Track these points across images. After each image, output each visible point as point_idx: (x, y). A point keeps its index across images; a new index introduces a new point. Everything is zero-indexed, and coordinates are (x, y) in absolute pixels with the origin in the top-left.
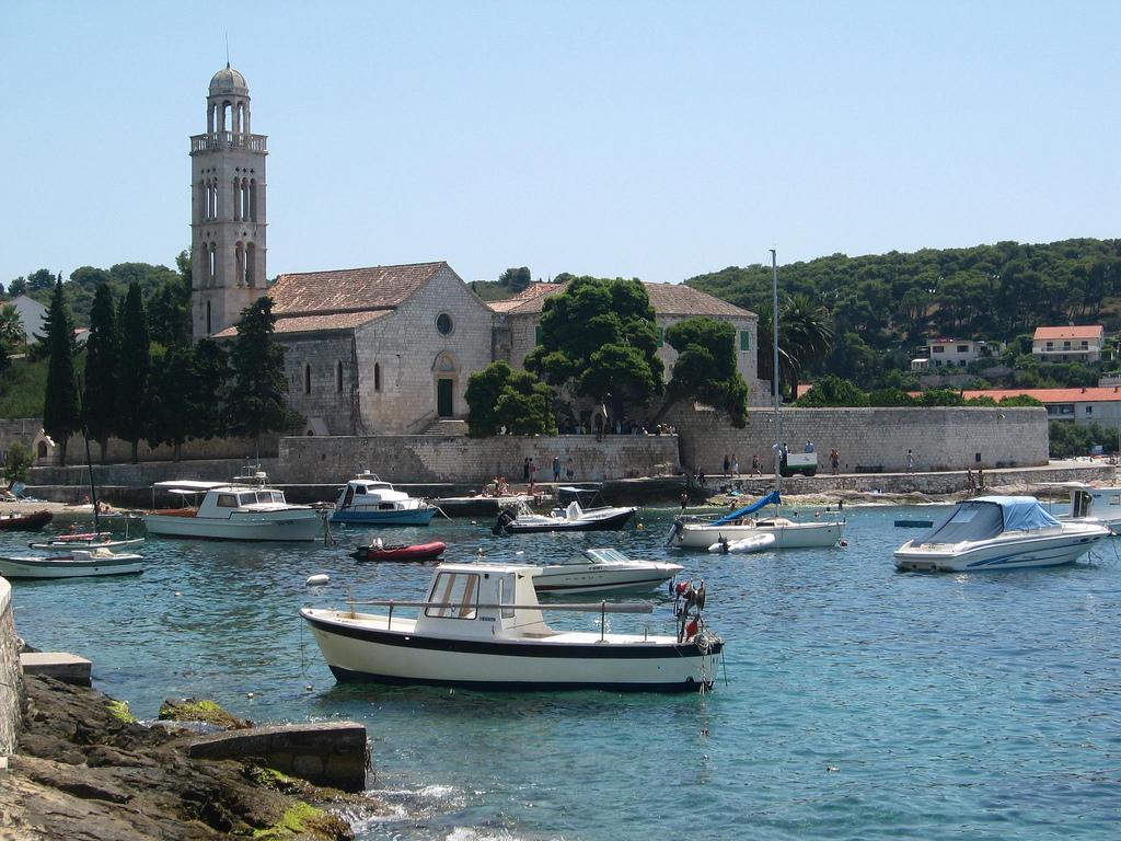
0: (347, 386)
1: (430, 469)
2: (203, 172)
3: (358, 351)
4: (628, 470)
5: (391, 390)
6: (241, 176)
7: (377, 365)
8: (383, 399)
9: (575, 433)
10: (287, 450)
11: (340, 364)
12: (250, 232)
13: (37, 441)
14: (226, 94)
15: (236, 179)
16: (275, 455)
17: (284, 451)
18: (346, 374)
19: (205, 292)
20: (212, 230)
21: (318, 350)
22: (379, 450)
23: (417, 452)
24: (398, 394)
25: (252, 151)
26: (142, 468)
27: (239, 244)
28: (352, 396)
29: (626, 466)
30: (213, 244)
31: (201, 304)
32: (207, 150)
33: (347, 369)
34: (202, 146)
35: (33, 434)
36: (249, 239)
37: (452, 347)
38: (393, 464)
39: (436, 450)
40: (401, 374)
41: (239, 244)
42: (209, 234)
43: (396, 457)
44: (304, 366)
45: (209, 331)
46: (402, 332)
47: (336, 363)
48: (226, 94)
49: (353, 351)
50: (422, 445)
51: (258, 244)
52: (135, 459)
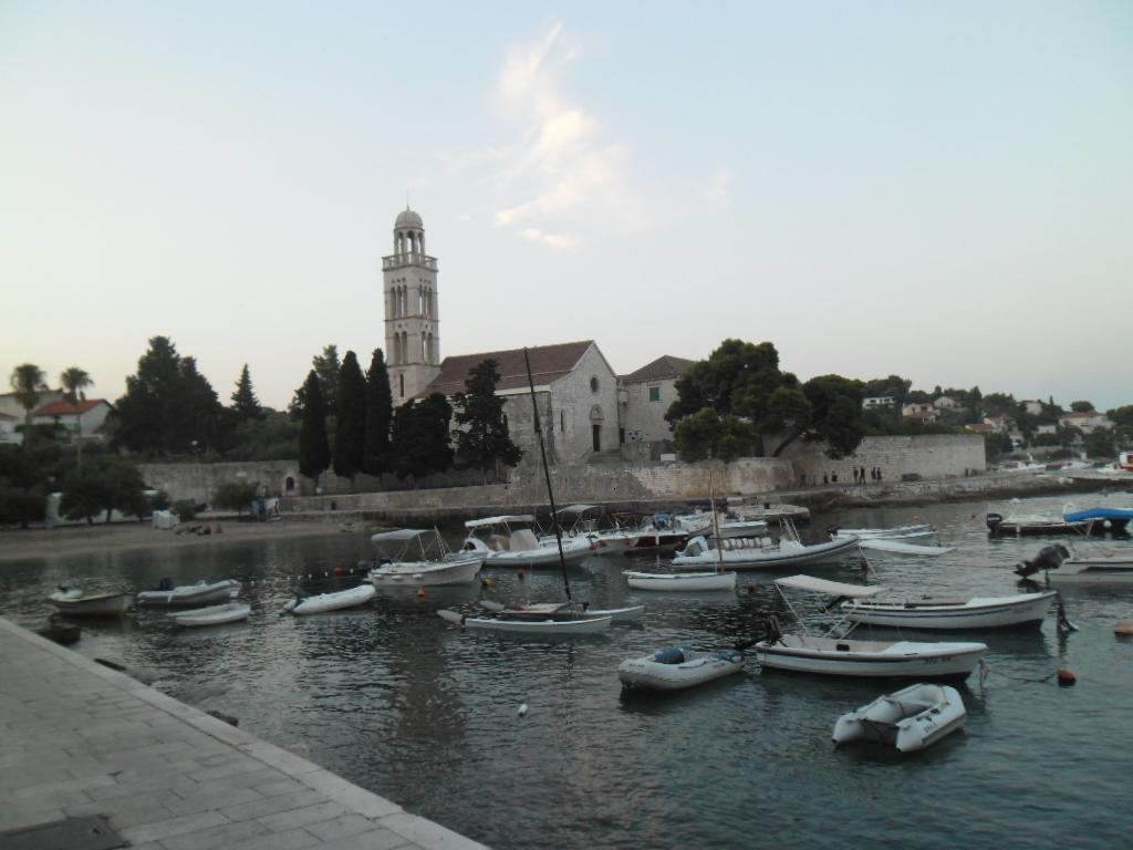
8: (566, 438)
9: (706, 458)
12: (430, 325)
14: (409, 230)
20: (403, 323)
25: (427, 267)
27: (423, 333)
32: (392, 266)
33: (543, 415)
34: (387, 266)
35: (281, 473)
36: (428, 330)
37: (599, 402)
43: (617, 479)
48: (409, 230)
49: (549, 403)
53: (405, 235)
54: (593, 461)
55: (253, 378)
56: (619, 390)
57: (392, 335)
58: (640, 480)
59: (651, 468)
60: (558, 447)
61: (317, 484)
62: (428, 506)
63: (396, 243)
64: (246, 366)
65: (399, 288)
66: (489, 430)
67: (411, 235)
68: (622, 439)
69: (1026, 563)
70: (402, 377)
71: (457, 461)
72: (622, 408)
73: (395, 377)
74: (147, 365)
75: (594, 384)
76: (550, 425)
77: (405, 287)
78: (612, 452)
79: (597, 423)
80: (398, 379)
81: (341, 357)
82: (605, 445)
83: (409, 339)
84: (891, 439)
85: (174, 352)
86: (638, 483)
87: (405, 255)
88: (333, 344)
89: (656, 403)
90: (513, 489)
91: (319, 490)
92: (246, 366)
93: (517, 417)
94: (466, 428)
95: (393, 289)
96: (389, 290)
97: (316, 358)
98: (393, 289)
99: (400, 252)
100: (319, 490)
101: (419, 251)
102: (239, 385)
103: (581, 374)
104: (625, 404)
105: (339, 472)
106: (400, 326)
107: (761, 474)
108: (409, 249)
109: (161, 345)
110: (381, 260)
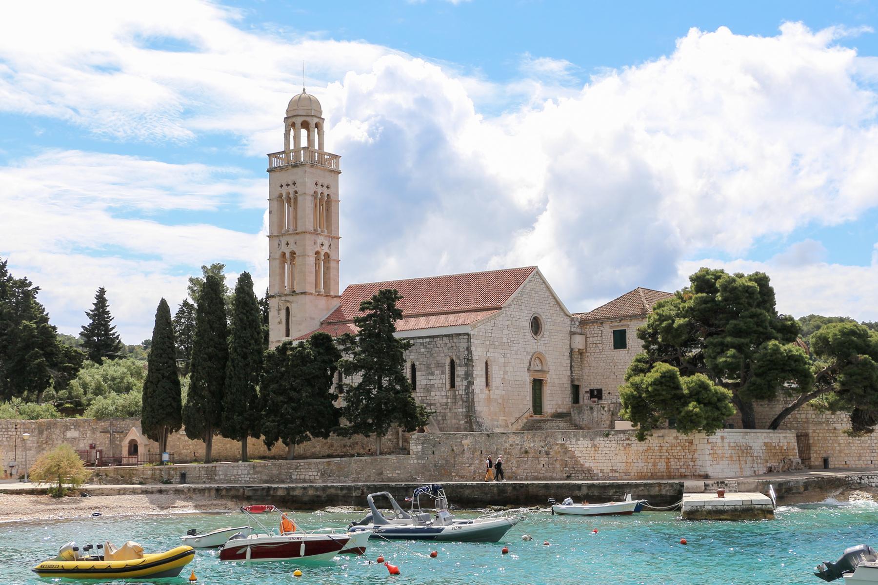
0: (460, 383)
1: (587, 465)
2: (281, 186)
3: (473, 349)
4: (769, 465)
5: (497, 388)
6: (320, 191)
10: (420, 447)
12: (326, 243)
16: (406, 451)
17: (415, 448)
18: (460, 371)
19: (283, 298)
20: (291, 240)
21: (425, 347)
22: (527, 445)
23: (570, 447)
24: (504, 393)
26: (254, 467)
27: (317, 253)
28: (467, 394)
29: (767, 462)
30: (293, 253)
31: (279, 310)
33: (460, 366)
34: (276, 163)
35: (123, 432)
36: (325, 249)
37: (541, 349)
38: (544, 460)
39: (595, 446)
40: (505, 373)
42: (288, 244)
45: (288, 335)
46: (505, 332)
47: (448, 361)
49: (469, 349)
50: (578, 440)
51: (333, 256)
52: (245, 458)
53: (298, 125)
54: (532, 427)
55: (112, 308)
56: (572, 333)
57: (278, 255)
58: (577, 454)
59: (592, 439)
60: (480, 407)
61: (163, 449)
62: (305, 481)
66: (385, 381)
67: (305, 125)
68: (576, 399)
69: (828, 565)
70: (288, 309)
71: (344, 423)
72: (576, 356)
75: (536, 325)
76: (469, 375)
77: (296, 192)
78: (558, 416)
79: (539, 376)
80: (283, 313)
81: (231, 283)
82: (549, 407)
83: (297, 260)
86: (573, 457)
87: (297, 151)
89: (622, 352)
90: (412, 461)
91: (166, 457)
92: (102, 291)
93: (428, 367)
94: (357, 379)
95: (281, 196)
96: (277, 194)
98: (281, 196)
99: (292, 147)
100: (166, 457)
101: (317, 147)
102: (92, 317)
104: (581, 353)
105: (191, 435)
107: (745, 451)
108: (304, 143)
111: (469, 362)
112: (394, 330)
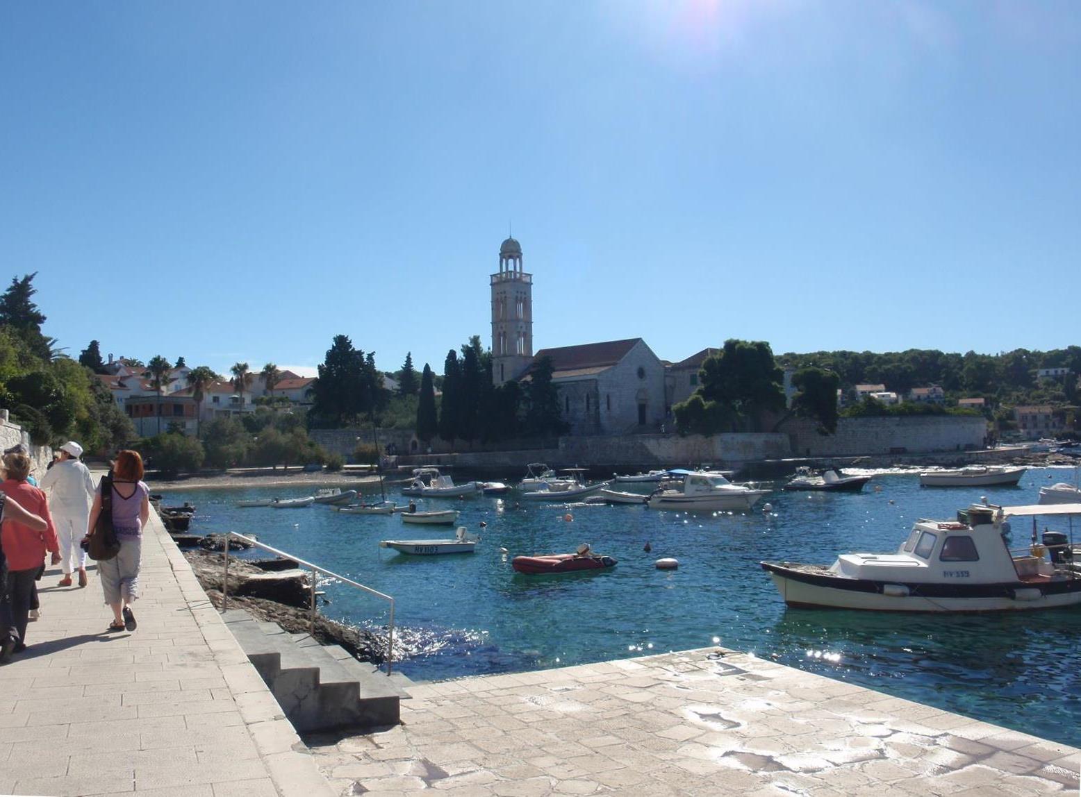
0: (592, 408)
2: (498, 294)
3: (599, 388)
4: (767, 453)
7: (608, 397)
11: (588, 395)
13: (411, 441)
15: (517, 297)
16: (557, 447)
17: (562, 445)
18: (592, 401)
23: (644, 443)
30: (505, 332)
35: (410, 437)
41: (519, 332)
43: (633, 447)
44: (565, 397)
47: (585, 395)
48: (510, 250)
56: (666, 376)
60: (604, 421)
63: (501, 261)
64: (409, 354)
65: (501, 299)
70: (502, 365)
73: (497, 365)
74: (331, 356)
75: (641, 373)
82: (650, 418)
84: (881, 419)
85: (351, 346)
86: (647, 450)
88: (477, 334)
92: (409, 354)
97: (463, 346)
98: (497, 299)
103: (628, 365)
106: (502, 327)
109: (342, 342)
110: (490, 277)
111: (597, 396)
112: (551, 378)
